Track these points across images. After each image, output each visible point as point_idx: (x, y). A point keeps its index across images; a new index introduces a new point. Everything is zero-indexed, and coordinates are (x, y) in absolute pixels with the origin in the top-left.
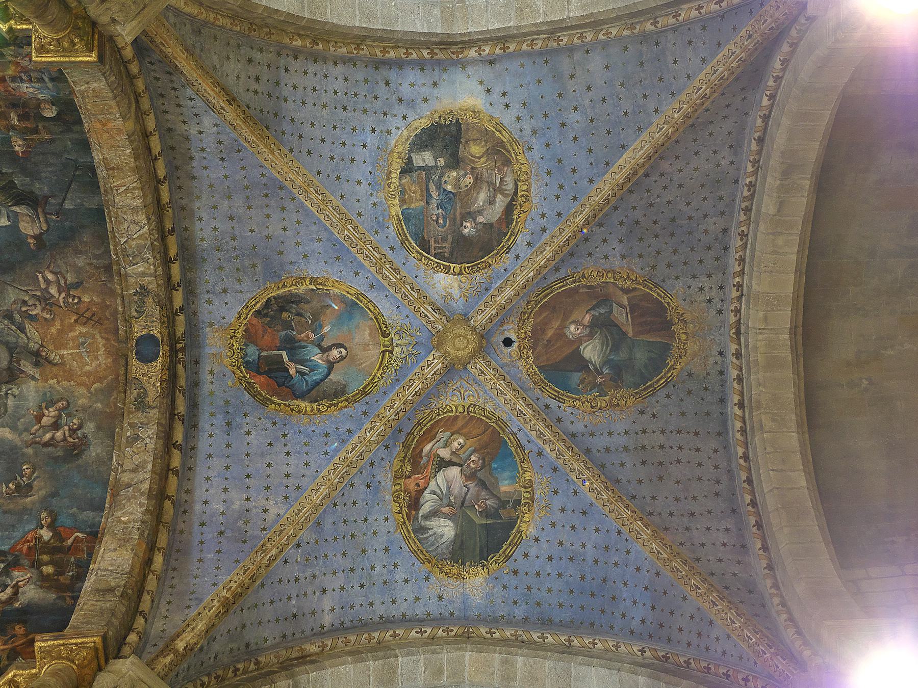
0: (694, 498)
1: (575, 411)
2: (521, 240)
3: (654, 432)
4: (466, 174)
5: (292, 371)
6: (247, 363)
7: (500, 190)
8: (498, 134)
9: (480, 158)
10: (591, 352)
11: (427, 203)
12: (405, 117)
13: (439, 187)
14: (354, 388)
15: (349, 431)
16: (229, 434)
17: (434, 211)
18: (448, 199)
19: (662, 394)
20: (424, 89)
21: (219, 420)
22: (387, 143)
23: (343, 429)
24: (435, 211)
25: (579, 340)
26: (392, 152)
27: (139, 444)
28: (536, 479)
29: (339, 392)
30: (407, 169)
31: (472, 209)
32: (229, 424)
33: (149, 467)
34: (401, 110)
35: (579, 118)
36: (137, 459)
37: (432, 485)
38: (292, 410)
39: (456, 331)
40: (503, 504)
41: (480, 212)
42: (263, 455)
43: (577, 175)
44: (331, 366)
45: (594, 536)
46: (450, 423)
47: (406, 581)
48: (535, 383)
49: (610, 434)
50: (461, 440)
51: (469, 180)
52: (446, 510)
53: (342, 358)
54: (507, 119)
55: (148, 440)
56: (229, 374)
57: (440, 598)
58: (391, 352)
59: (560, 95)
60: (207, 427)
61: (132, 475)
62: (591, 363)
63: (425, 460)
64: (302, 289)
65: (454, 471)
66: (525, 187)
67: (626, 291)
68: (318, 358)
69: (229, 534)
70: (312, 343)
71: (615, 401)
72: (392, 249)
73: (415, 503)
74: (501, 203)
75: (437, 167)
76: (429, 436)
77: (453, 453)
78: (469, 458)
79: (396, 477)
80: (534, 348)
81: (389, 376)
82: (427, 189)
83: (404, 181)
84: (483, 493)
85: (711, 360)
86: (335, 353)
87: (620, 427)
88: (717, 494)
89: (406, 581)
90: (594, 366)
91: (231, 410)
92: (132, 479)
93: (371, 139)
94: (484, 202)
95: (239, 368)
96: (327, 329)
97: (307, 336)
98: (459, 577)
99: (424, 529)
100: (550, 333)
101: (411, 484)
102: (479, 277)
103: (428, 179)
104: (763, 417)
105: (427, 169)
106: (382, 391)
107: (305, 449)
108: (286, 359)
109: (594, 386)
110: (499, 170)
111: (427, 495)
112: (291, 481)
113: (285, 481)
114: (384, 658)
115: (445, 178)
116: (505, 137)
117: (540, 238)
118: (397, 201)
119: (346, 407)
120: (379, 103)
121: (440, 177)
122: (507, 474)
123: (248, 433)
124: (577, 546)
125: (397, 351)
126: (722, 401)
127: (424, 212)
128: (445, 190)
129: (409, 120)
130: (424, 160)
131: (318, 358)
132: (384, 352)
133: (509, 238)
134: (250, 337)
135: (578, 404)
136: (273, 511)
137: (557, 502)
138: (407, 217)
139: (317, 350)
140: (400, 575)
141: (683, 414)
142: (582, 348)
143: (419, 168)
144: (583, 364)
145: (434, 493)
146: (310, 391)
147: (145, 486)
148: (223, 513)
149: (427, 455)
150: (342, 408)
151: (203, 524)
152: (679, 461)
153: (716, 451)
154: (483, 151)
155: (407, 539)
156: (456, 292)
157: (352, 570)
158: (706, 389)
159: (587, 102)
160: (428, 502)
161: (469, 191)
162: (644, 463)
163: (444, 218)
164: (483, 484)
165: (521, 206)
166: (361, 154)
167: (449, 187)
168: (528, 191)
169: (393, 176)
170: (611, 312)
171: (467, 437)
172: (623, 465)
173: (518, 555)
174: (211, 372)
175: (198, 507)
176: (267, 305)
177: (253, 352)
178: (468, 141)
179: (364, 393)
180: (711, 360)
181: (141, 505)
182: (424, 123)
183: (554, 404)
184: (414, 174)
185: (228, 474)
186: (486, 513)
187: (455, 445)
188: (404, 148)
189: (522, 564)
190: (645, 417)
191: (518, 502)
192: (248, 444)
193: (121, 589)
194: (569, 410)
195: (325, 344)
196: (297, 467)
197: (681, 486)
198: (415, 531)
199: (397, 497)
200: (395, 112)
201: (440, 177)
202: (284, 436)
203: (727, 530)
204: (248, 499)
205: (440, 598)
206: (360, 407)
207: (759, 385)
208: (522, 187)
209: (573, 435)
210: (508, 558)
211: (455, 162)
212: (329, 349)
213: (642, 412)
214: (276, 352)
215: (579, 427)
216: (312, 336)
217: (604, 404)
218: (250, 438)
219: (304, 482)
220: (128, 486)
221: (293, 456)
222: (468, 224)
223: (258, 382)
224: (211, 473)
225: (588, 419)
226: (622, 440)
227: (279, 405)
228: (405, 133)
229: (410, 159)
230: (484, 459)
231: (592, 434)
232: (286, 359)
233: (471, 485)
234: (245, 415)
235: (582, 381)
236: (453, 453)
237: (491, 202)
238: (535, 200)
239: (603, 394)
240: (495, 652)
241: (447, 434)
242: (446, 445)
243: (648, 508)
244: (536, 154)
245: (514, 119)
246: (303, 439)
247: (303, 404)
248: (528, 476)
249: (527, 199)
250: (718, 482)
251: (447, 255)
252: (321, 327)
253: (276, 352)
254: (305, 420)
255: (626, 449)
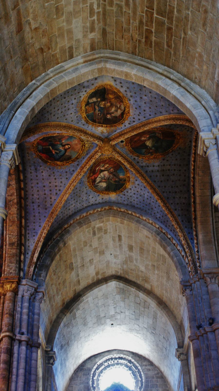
0: (177, 187)
1: (143, 160)
2: (127, 123)
3: (167, 165)
4: (107, 103)
5: (54, 152)
6: (40, 151)
7: (120, 108)
8: (119, 93)
9: (112, 99)
10: (149, 143)
11: (95, 111)
12: (86, 91)
13: (98, 106)
14: (74, 157)
15: (73, 171)
16: (36, 173)
17: (97, 112)
18: (101, 109)
19: (170, 155)
20: (92, 81)
21: (33, 168)
22: (80, 100)
23: (71, 170)
24: (97, 112)
25: (145, 141)
26: (82, 101)
27: (11, 187)
28: (131, 176)
29: (69, 158)
30: (88, 104)
31: (110, 112)
32: (36, 169)
33: (15, 194)
34: (85, 89)
35: (147, 98)
36: (11, 192)
37: (99, 176)
38: (55, 164)
39: (105, 149)
40: (120, 180)
41: (113, 113)
42: (48, 179)
43: (145, 112)
44: (66, 150)
45: (147, 193)
46: (104, 162)
47: (93, 197)
48: (131, 152)
49: (154, 166)
50: (108, 165)
51: (109, 104)
52: (104, 181)
53: (69, 148)
54: (122, 90)
55: (13, 185)
56: (33, 153)
57: (103, 199)
58: (85, 146)
59: (140, 90)
60: (29, 170)
61: (11, 197)
62: (148, 146)
63: (97, 171)
64: (55, 135)
65: (106, 173)
66: (128, 110)
67: (160, 131)
68: (61, 148)
69: (41, 206)
70: (59, 144)
71: (155, 157)
72: (84, 125)
73: (94, 181)
74: (119, 112)
75: (97, 101)
76: (98, 165)
77: (105, 168)
78: (110, 169)
79: (88, 178)
80: (130, 143)
81: (85, 153)
82: (95, 107)
83: (86, 107)
84: (115, 177)
85: (187, 144)
86: (67, 147)
87: (156, 164)
88: (184, 185)
89: (93, 197)
90: (150, 147)
91: (36, 165)
92: (11, 198)
93: (74, 101)
94: (114, 111)
95: (36, 152)
96: (63, 141)
97: (58, 143)
98: (108, 194)
99: (98, 186)
100: (135, 140)
101: (93, 178)
102: (112, 128)
103: (95, 105)
104: (200, 172)
105: (95, 103)
106: (82, 158)
107: (61, 177)
108: (51, 149)
109: (149, 153)
110: (119, 103)
111: (98, 179)
112: (57, 188)
113: (56, 188)
114: (88, 223)
115: (100, 104)
116: (121, 95)
117: (133, 123)
118: (84, 113)
119: (71, 163)
120: (77, 90)
121: (99, 104)
122: (122, 174)
123: (42, 172)
124: (142, 193)
125: (87, 145)
126: (189, 155)
127: (94, 113)
128: (100, 107)
129: (87, 92)
130: (93, 100)
131: (61, 148)
132: (82, 146)
133: (122, 121)
134: (38, 144)
135: (144, 158)
136: (53, 198)
137: (137, 183)
138: (88, 116)
139: (61, 146)
140: (91, 197)
141: (176, 160)
142: (146, 143)
143: (92, 103)
144: (146, 147)
145: (100, 177)
146: (60, 158)
147: (15, 201)
148: (38, 199)
149: (98, 170)
150: (70, 164)
151: (33, 203)
152: (174, 175)
153: (185, 170)
154: (114, 97)
155: (92, 189)
156: (105, 131)
157: (77, 201)
158: (184, 152)
159: (149, 96)
160: (98, 180)
161: (109, 107)
162: (163, 175)
163: (101, 114)
164: (114, 175)
165: (127, 114)
166: (71, 106)
167: (102, 106)
168: (129, 111)
169: (83, 107)
170: (156, 134)
171: (109, 164)
172: (157, 176)
173: (125, 191)
174: (28, 153)
175: (31, 197)
176: (44, 138)
177: (40, 147)
178: (108, 94)
179: (77, 158)
180: (187, 144)
181: (16, 208)
182: (93, 91)
183: (136, 158)
184: (90, 105)
185: (38, 186)
186: (115, 181)
187: (106, 166)
188: (86, 100)
189: (126, 193)
190: (165, 161)
191: (125, 180)
192: (43, 176)
193: (16, 243)
194: (141, 159)
195: (63, 144)
196: (59, 183)
197: (174, 183)
198: (94, 187)
199: (89, 182)
200: (82, 91)
201: (99, 104)
202: (54, 173)
203: (185, 198)
204: (45, 194)
205: (103, 199)
206: (76, 163)
207: (200, 161)
208: (127, 110)
209: (142, 167)
210: (122, 191)
211: (104, 99)
212: (65, 145)
213: (164, 160)
214: (47, 147)
215: (144, 164)
216: (59, 143)
217: (152, 158)
218: (43, 174)
219: (61, 188)
220: (10, 201)
221: (57, 180)
222: (109, 116)
223: (43, 156)
224: (33, 185)
225: (147, 162)
226: (157, 168)
227: (51, 163)
228: (86, 95)
229: (88, 102)
230: (115, 170)
231: (148, 166)
232: (51, 149)
233: (111, 175)
234: (41, 166)
235: (146, 151)
236: (105, 168)
237: (116, 111)
238: (131, 114)
239: (152, 155)
240: (118, 218)
241: (103, 164)
242: (103, 167)
243: (163, 190)
244: (132, 101)
245: (124, 91)
246: (59, 174)
247: (58, 163)
248: (128, 175)
249: (129, 113)
250: (185, 181)
251: (102, 123)
252: (62, 141)
253: (47, 147)
254: (59, 168)
255: (158, 171)
